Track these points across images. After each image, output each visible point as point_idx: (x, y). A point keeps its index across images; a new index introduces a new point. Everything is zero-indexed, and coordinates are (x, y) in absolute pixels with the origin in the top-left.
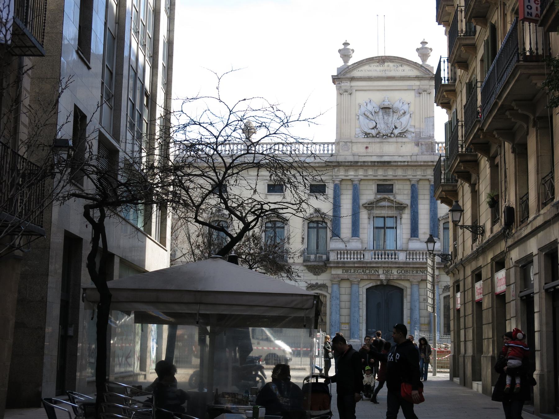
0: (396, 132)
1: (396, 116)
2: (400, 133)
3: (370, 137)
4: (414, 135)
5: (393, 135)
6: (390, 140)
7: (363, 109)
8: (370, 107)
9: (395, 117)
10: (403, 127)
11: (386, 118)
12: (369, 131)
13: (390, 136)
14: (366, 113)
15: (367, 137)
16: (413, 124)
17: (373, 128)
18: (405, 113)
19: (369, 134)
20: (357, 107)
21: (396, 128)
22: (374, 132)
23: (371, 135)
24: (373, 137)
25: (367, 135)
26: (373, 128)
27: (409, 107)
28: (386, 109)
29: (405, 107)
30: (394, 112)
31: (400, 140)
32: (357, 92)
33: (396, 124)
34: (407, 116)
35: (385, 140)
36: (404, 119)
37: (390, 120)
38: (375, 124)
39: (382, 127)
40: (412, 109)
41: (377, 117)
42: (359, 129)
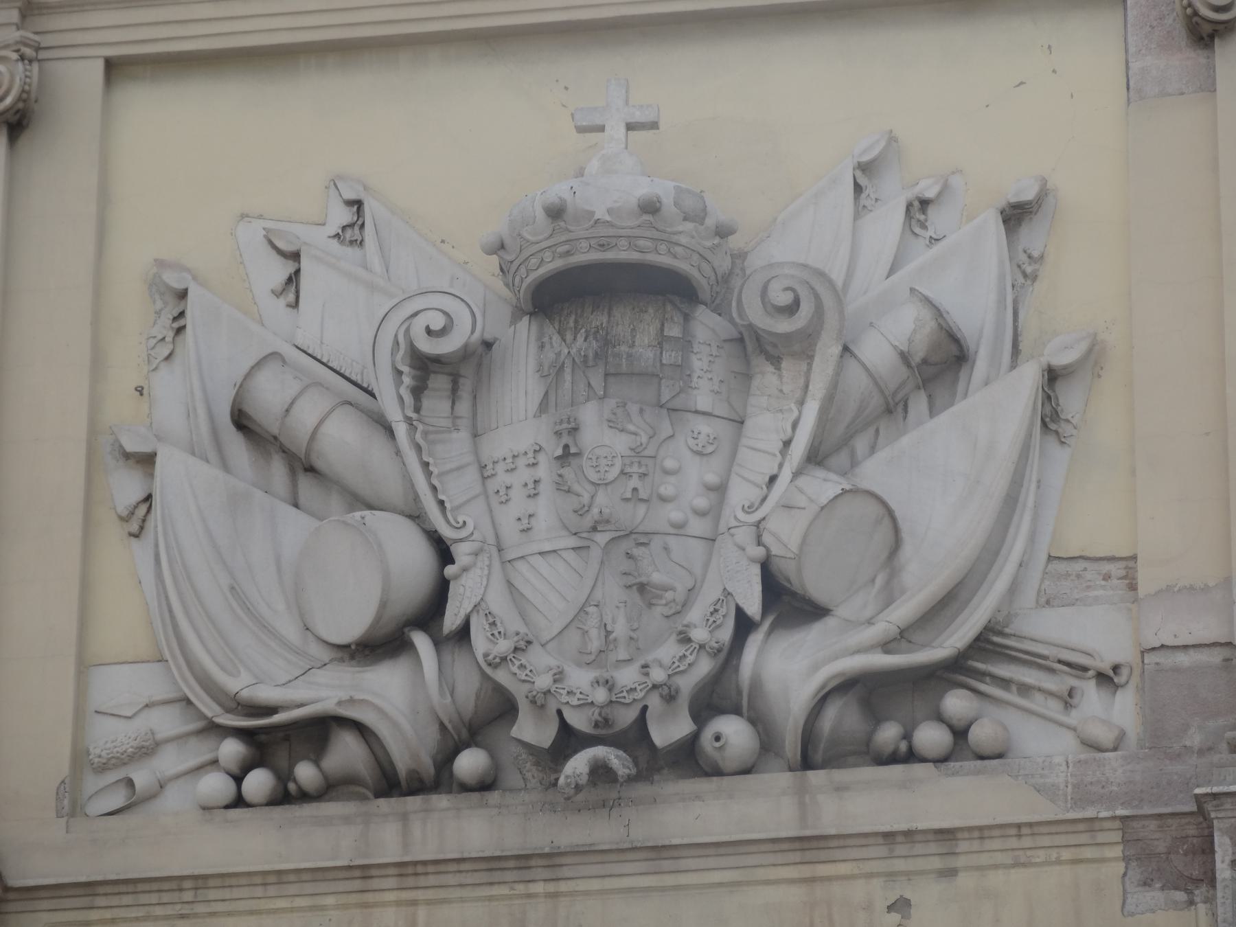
0: (791, 669)
1: (783, 414)
2: (870, 691)
3: (330, 789)
4: (1120, 712)
5: (733, 733)
6: (688, 813)
7: (221, 351)
8: (346, 319)
9: (765, 428)
10: (922, 582)
11: (600, 436)
12: (325, 690)
13: (689, 759)
14: (270, 395)
15: (284, 796)
16: (1093, 524)
17: (381, 646)
18: (943, 363)
19: (318, 731)
20: (134, 318)
21: (787, 603)
22: (399, 701)
23: (346, 753)
24: (390, 784)
25: (279, 748)
26: (381, 646)
27: (1026, 271)
28: (603, 293)
29: (966, 279)
30: (753, 349)
31: (864, 801)
32: (159, 121)
33: (786, 534)
34: (997, 405)
35: (600, 831)
36: (942, 475)
37: (690, 479)
38: (410, 559)
39: (542, 607)
40: (1080, 295)
41: (456, 447)
42: (146, 683)
